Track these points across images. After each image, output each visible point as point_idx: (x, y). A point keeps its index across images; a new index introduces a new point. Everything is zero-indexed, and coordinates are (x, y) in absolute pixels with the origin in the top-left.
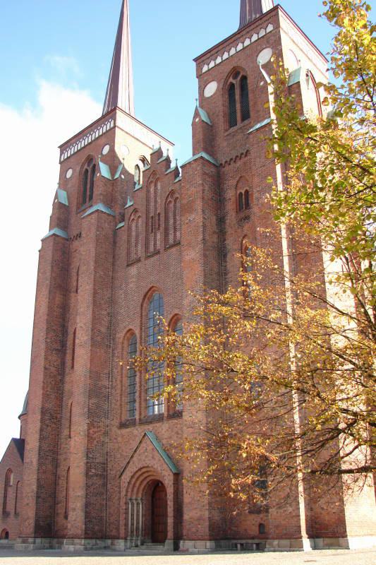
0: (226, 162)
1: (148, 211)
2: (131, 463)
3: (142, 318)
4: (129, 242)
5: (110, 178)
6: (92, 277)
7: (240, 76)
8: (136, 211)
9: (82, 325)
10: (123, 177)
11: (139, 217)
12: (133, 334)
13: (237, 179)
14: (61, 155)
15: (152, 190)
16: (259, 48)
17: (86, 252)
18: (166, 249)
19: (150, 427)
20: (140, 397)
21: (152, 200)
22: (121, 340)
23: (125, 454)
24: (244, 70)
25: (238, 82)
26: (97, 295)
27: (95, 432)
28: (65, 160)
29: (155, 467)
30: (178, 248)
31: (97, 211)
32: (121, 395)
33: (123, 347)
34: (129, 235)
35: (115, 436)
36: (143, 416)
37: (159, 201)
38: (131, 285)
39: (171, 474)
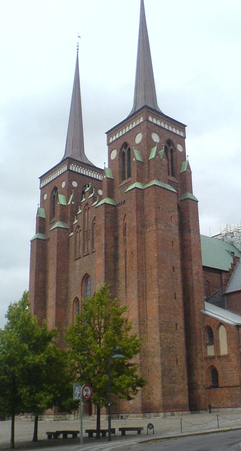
0: (119, 203)
1: (84, 227)
3: (82, 291)
4: (75, 245)
5: (66, 204)
8: (78, 227)
10: (73, 203)
11: (80, 230)
12: (78, 300)
16: (136, 131)
17: (53, 251)
21: (86, 220)
31: (58, 227)
33: (73, 307)
34: (76, 241)
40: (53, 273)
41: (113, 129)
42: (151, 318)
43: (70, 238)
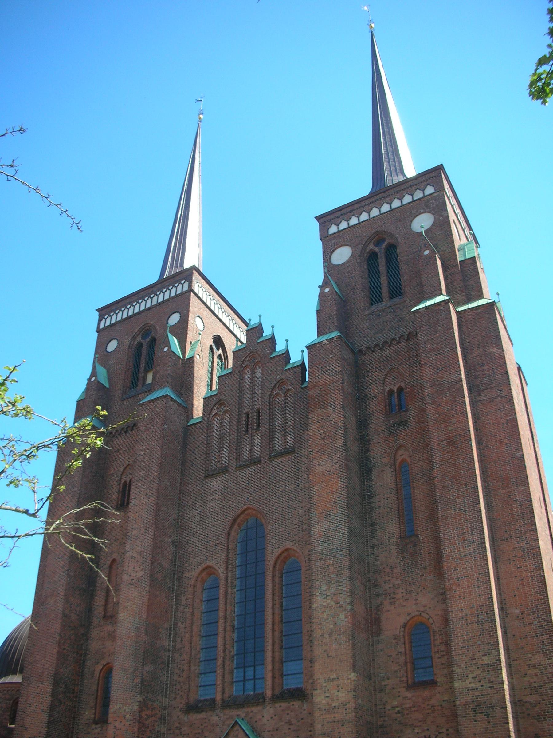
1: (240, 403)
3: (228, 552)
4: (208, 444)
6: (155, 485)
7: (386, 243)
9: (135, 555)
11: (226, 412)
13: (387, 371)
14: (100, 321)
15: (247, 377)
18: (270, 458)
19: (242, 712)
20: (224, 666)
22: (192, 582)
24: (391, 235)
25: (383, 250)
26: (160, 513)
27: (149, 716)
28: (106, 328)
30: (292, 457)
32: (190, 662)
33: (194, 592)
34: (209, 436)
35: (177, 725)
36: (227, 695)
37: (258, 392)
38: (212, 504)
40: (146, 501)
41: (340, 210)
42: (517, 611)
43: (190, 428)
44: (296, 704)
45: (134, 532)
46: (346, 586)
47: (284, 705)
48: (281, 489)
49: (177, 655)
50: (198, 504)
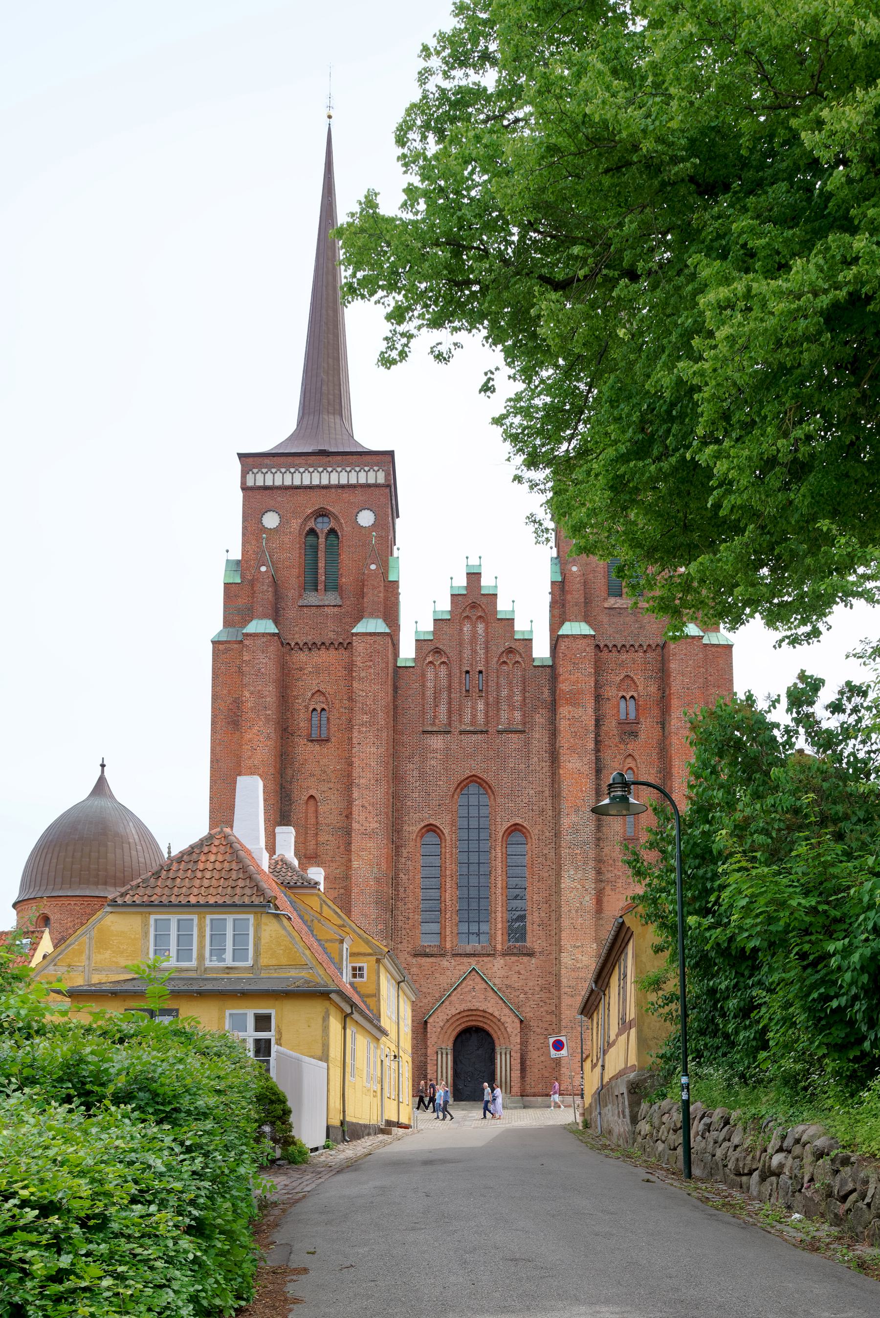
2: (447, 1003)
15: (467, 628)
23: (425, 990)
29: (490, 1011)
30: (522, 736)
39: (517, 1021)
43: (401, 670)
44: (526, 959)
45: (362, 781)
46: (592, 874)
47: (514, 958)
48: (512, 765)
49: (400, 904)
50: (416, 759)
